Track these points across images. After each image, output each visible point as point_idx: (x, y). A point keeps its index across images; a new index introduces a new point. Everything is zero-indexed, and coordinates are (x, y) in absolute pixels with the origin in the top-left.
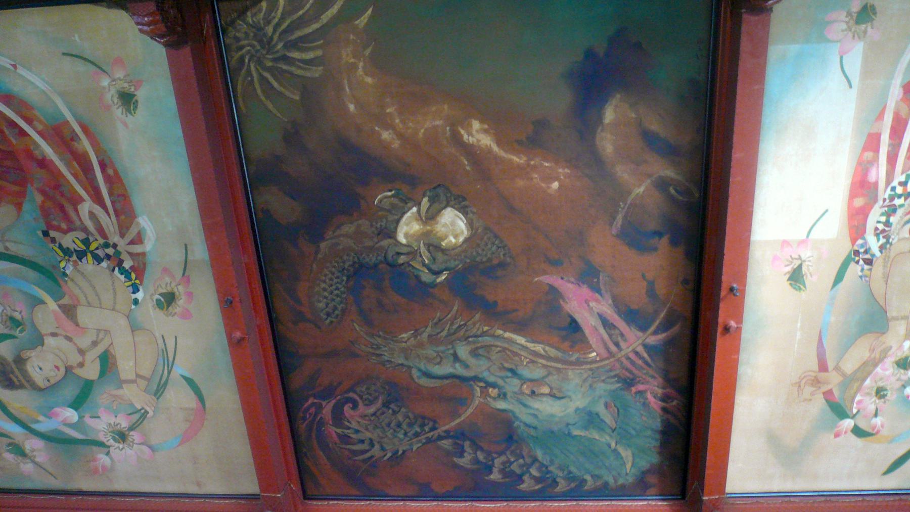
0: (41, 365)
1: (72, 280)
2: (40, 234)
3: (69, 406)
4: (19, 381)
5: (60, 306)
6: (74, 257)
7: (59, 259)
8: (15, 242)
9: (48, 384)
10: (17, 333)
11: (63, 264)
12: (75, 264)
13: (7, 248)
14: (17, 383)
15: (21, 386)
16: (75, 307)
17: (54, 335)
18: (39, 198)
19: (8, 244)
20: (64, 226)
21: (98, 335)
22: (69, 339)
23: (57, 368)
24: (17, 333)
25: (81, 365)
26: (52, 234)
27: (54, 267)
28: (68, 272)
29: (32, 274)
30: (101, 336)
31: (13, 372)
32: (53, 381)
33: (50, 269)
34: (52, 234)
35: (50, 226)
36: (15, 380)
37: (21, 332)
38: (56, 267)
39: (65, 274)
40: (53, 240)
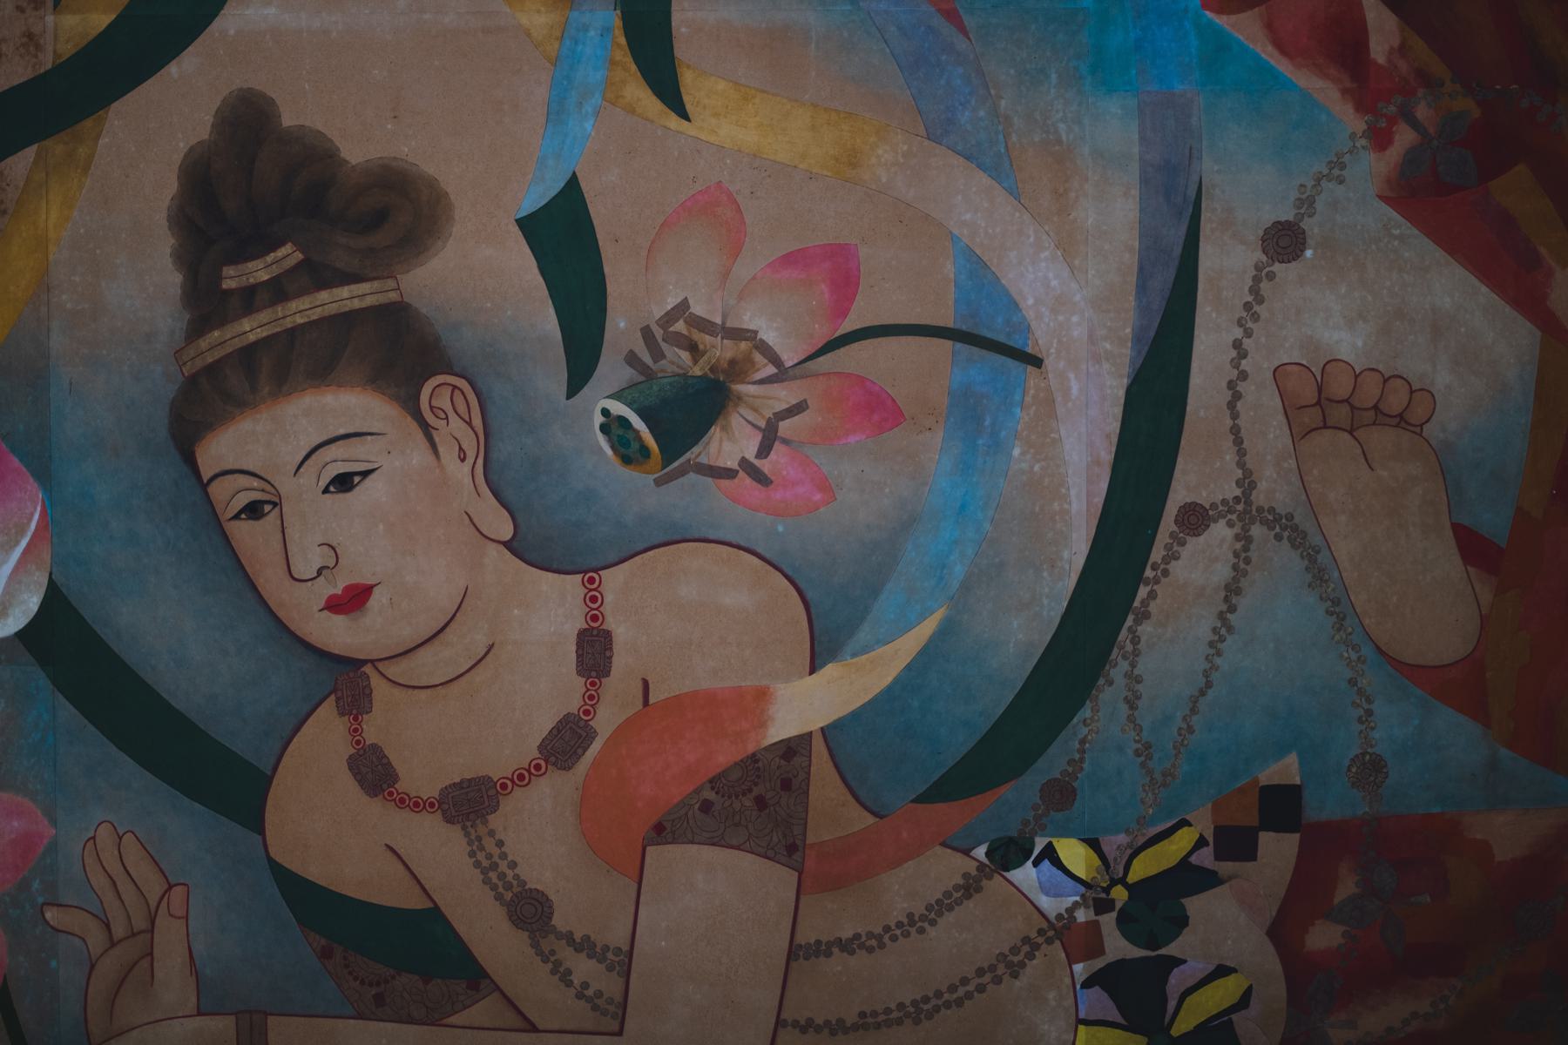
0: (370, 492)
1: (970, 887)
2: (1286, 769)
3: (54, 597)
4: (249, 299)
5: (794, 749)
6: (1117, 947)
7: (1114, 842)
8: (1232, 590)
9: (231, 495)
10: (604, 398)
11: (1074, 854)
12: (1069, 936)
13: (1195, 519)
14: (232, 278)
15: (207, 305)
16: (790, 851)
17: (594, 650)
18: (1507, 834)
19: (1221, 533)
20: (1323, 937)
21: (585, 946)
22: (565, 743)
23: (353, 600)
24: (604, 398)
25: (374, 773)
26: (1278, 851)
27: (1060, 794)
28: (1026, 875)
29: (1023, 625)
30: (583, 968)
31: (316, 275)
32: (245, 534)
33: (1053, 763)
34: (1278, 851)
35: (1324, 845)
36: (259, 271)
37: (614, 427)
38: (1060, 794)
39: (1009, 852)
40: (1235, 843)
